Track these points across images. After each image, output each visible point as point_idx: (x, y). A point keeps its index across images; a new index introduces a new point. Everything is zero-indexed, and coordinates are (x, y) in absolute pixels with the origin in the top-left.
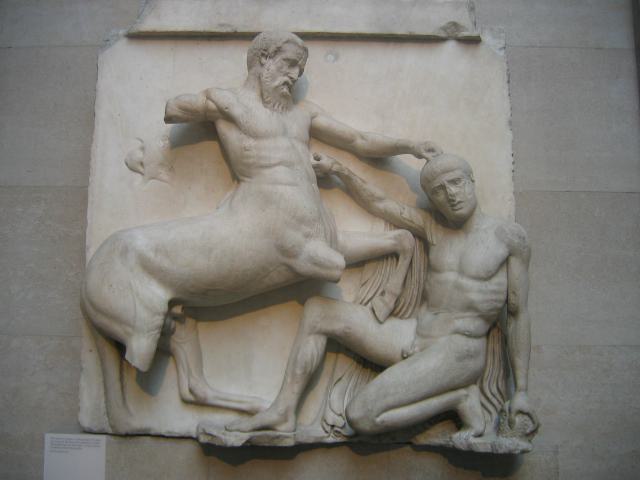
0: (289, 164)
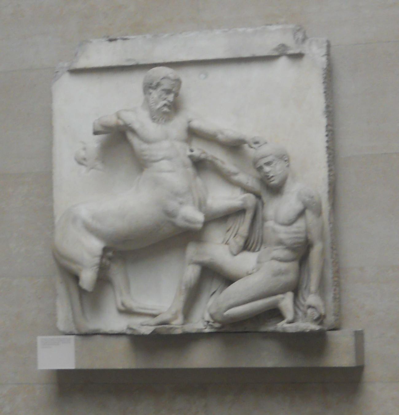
0: (169, 158)
